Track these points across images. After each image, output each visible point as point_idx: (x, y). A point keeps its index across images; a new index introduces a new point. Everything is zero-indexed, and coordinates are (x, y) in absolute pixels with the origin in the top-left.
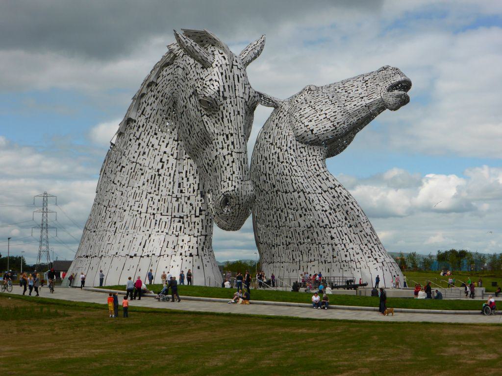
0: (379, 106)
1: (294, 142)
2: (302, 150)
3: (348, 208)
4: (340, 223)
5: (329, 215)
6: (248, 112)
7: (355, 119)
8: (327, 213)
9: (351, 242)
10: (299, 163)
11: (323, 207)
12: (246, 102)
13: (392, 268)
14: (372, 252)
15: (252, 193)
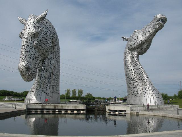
0: (153, 30)
1: (128, 51)
2: (130, 53)
3: (139, 72)
4: (137, 78)
5: (134, 76)
6: (31, 37)
7: (145, 37)
8: (133, 75)
9: (139, 85)
10: (128, 58)
11: (132, 73)
12: (29, 33)
13: (152, 96)
14: (145, 89)
15: (24, 66)
